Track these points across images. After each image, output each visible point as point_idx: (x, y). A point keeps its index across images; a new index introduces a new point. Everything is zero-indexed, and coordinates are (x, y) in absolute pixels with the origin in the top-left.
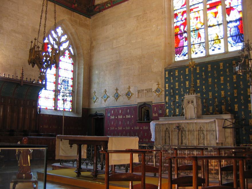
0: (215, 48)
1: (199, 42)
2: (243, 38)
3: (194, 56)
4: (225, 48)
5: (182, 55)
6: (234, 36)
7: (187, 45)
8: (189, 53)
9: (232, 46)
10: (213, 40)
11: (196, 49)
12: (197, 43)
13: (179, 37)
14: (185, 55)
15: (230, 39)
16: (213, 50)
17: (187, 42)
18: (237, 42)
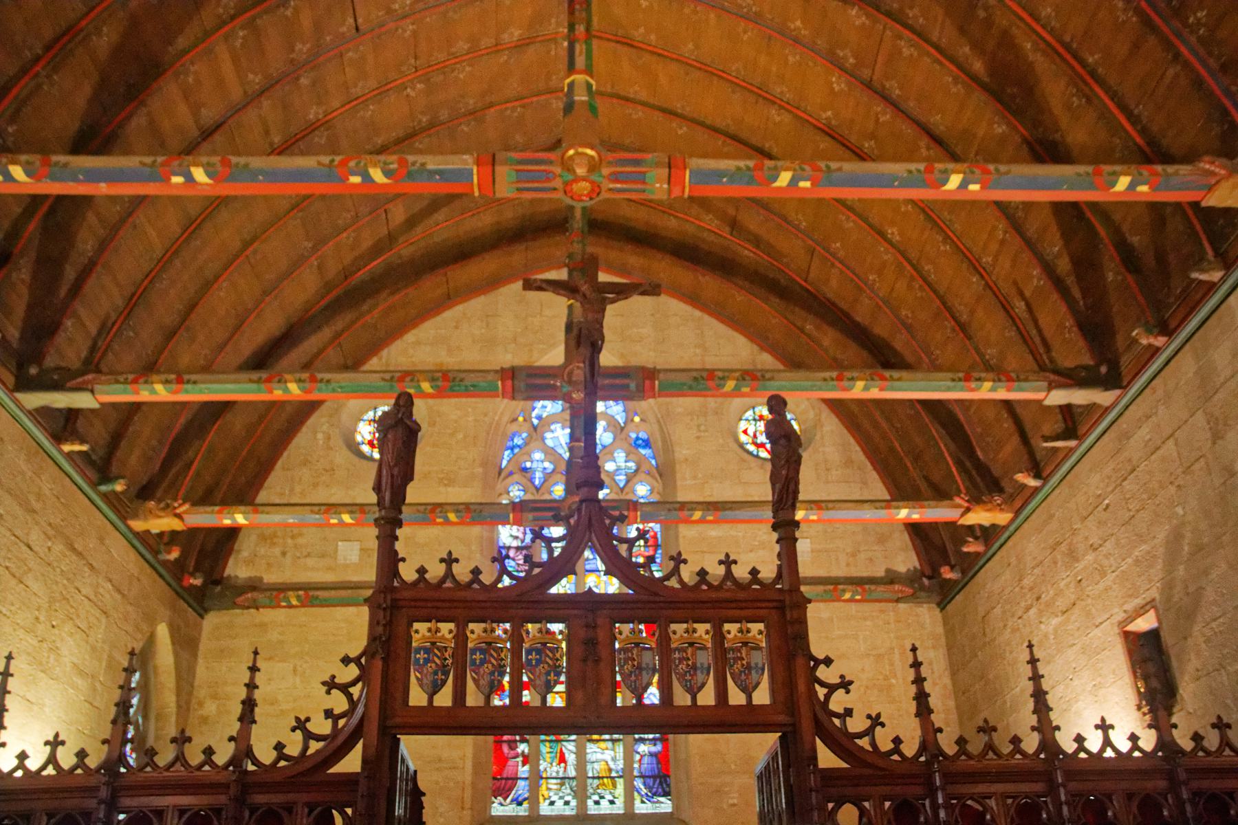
0: (602, 797)
1: (561, 775)
2: (668, 785)
3: (545, 809)
4: (625, 802)
5: (512, 801)
6: (649, 777)
7: (526, 775)
8: (534, 799)
9: (643, 802)
10: (599, 778)
11: (551, 794)
12: (554, 775)
13: (505, 749)
14: (520, 804)
15: (639, 783)
16: (597, 803)
17: (527, 768)
18: (655, 794)
